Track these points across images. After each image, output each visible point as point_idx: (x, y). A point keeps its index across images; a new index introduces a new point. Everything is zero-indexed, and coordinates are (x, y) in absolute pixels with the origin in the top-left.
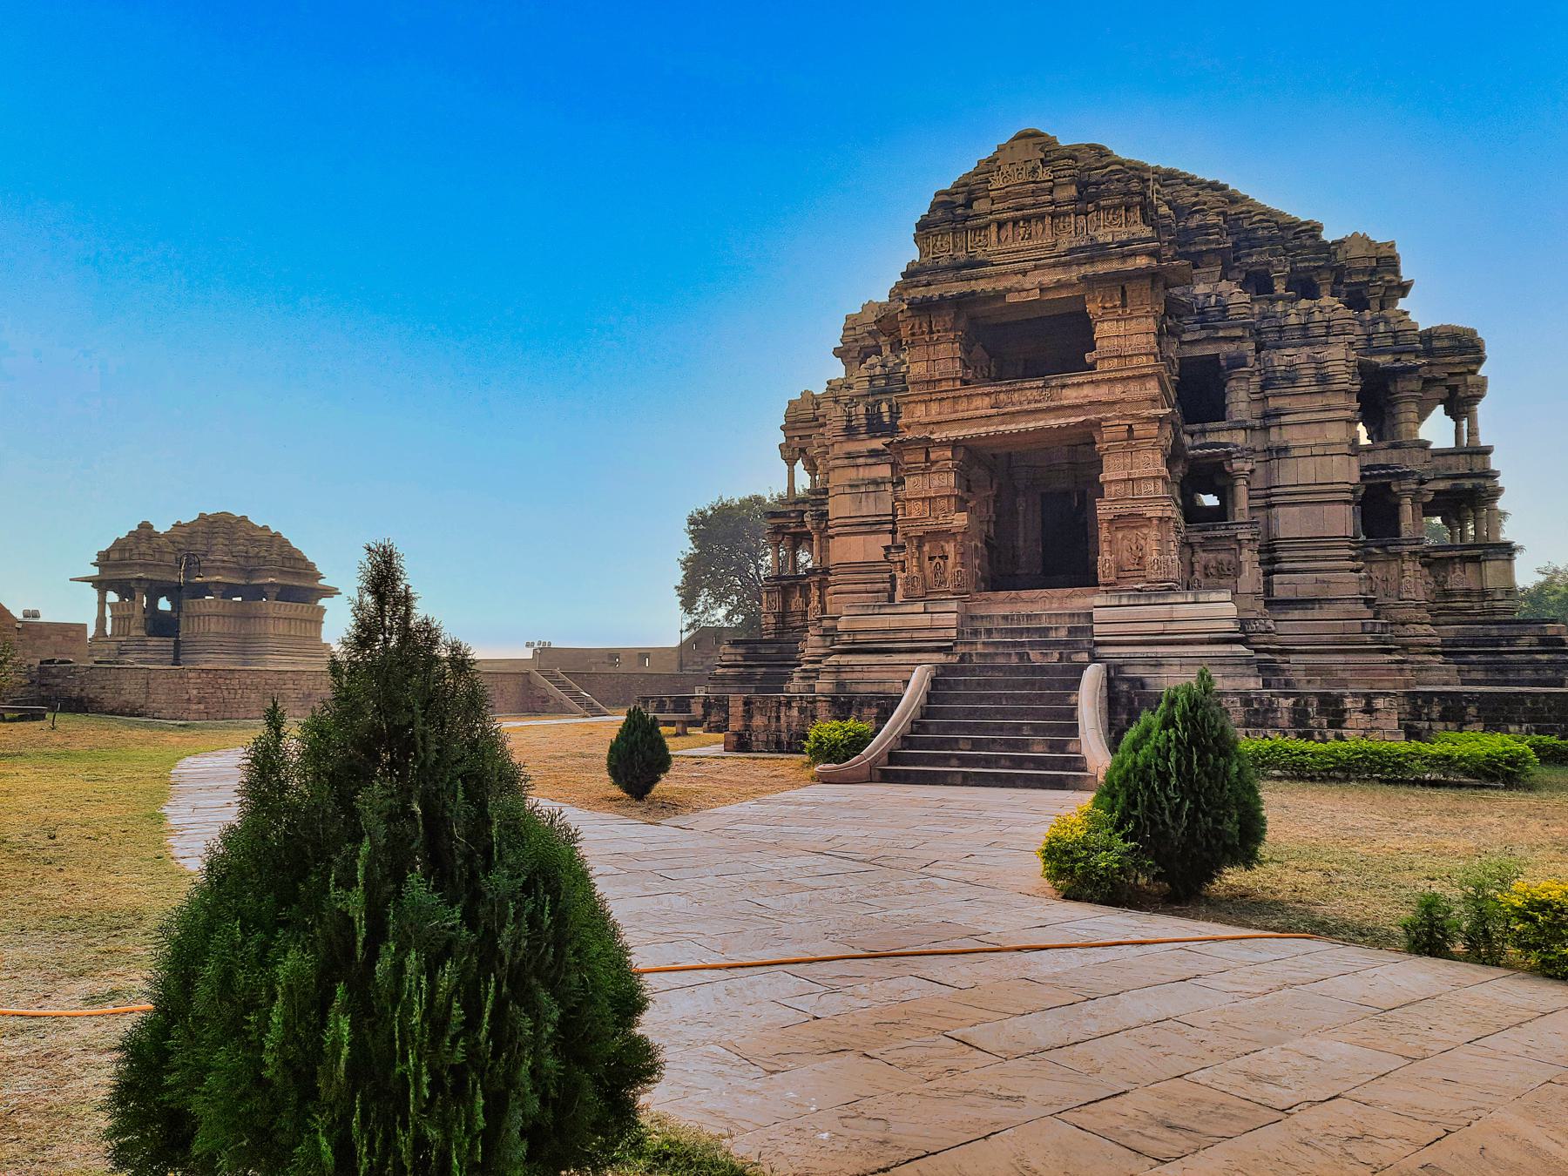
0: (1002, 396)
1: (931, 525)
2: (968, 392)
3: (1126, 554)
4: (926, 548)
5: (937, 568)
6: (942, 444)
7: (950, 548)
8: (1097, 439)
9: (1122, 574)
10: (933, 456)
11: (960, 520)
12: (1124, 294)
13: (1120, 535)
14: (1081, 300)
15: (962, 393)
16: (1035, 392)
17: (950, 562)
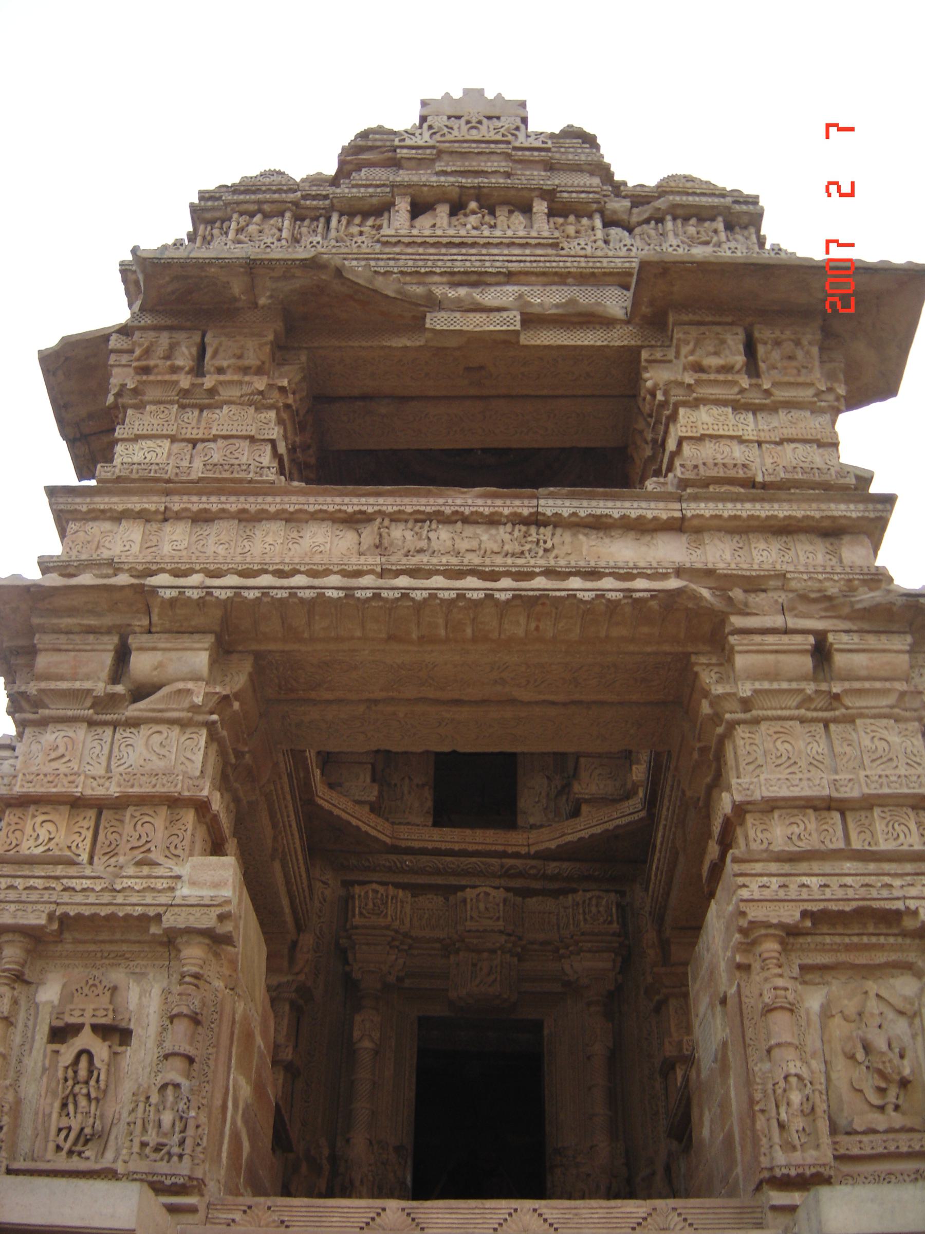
0: (397, 532)
1: (91, 888)
2: (292, 503)
3: (842, 1072)
4: (49, 993)
5: (81, 1083)
6: (181, 618)
7: (144, 999)
8: (708, 678)
9: (851, 1146)
10: (142, 664)
11: (208, 883)
12: (750, 349)
13: (814, 1001)
14: (629, 363)
15: (272, 504)
16: (502, 532)
17: (140, 1061)
